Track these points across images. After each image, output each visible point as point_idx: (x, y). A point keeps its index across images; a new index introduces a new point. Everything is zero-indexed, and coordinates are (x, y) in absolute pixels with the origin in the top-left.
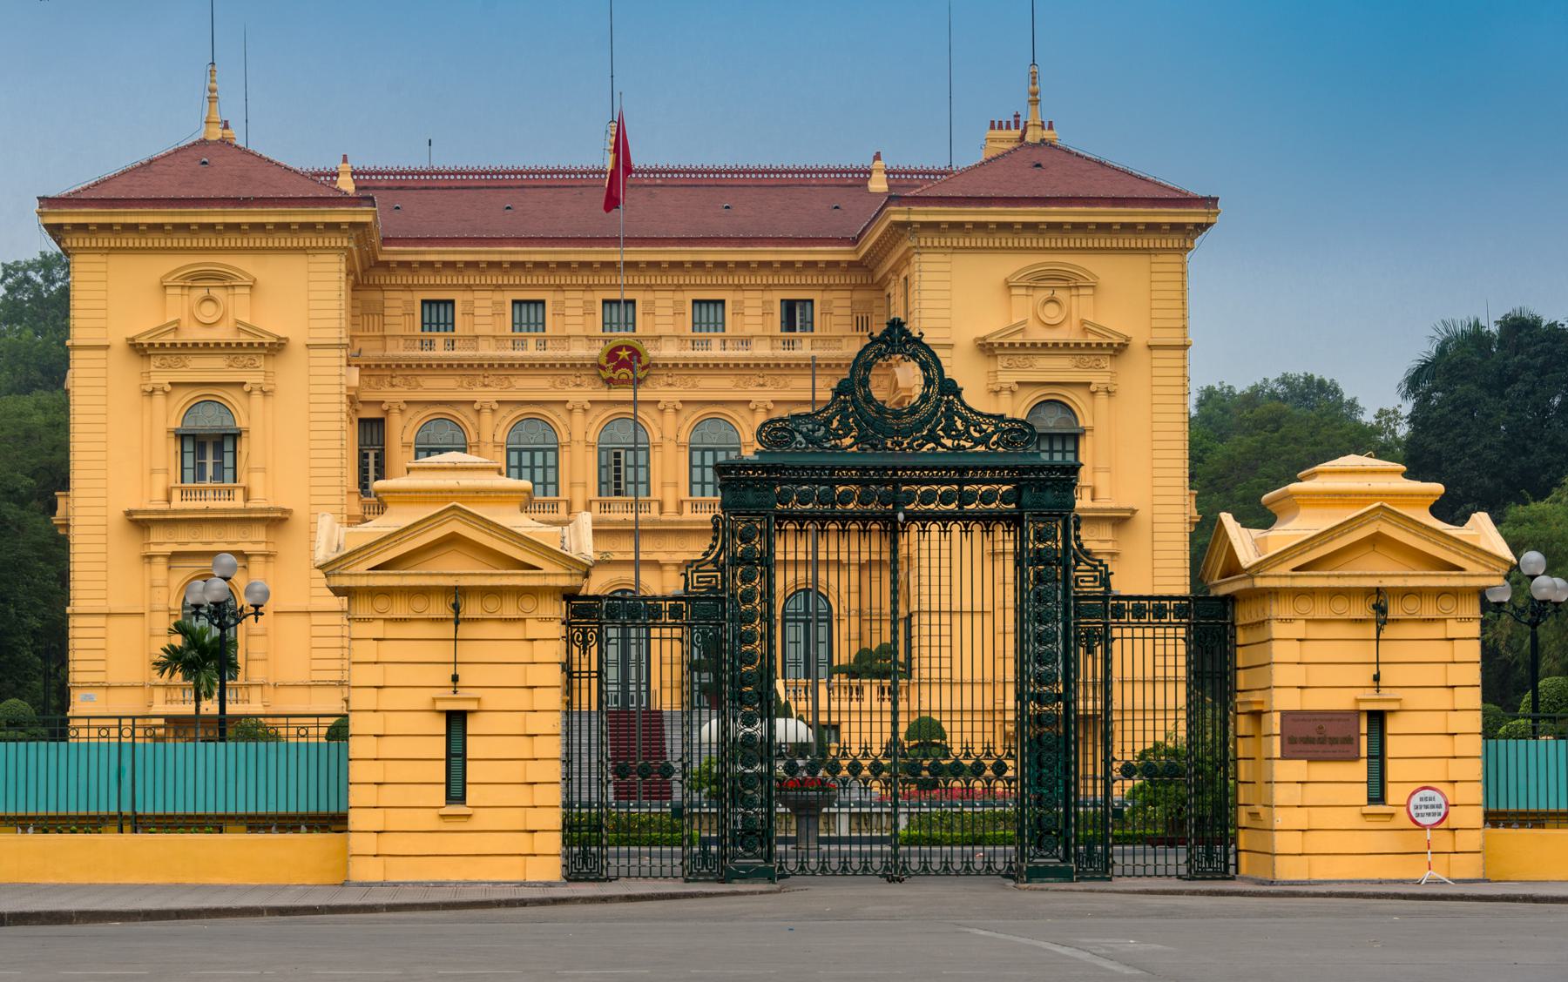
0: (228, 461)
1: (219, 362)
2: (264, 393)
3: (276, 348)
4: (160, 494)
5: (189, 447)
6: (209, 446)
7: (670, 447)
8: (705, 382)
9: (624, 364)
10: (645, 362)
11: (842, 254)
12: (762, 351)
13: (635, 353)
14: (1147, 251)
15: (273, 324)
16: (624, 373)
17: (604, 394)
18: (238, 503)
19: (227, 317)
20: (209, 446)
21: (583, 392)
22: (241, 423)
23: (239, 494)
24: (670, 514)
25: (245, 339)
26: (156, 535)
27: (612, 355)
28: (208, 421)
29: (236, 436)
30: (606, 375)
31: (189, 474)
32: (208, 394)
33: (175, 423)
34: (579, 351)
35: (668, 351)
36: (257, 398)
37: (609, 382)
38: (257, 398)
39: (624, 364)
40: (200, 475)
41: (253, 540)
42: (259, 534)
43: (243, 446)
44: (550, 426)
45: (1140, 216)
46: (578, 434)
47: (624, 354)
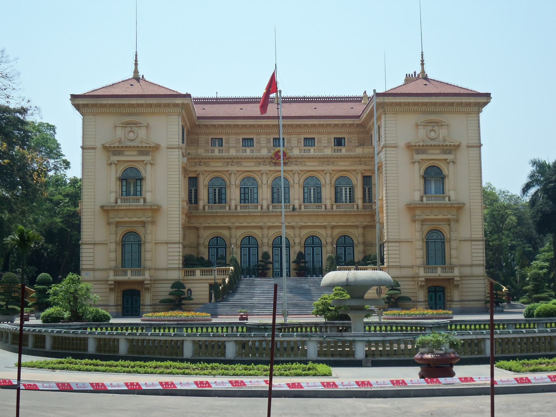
0: (139, 188)
2: (151, 164)
4: (112, 200)
5: (124, 184)
8: (308, 164)
10: (288, 156)
11: (357, 121)
12: (328, 152)
30: (274, 161)
31: (124, 193)
34: (264, 152)
35: (296, 152)
36: (149, 166)
38: (149, 166)
43: (144, 183)
44: (254, 179)
46: (265, 182)
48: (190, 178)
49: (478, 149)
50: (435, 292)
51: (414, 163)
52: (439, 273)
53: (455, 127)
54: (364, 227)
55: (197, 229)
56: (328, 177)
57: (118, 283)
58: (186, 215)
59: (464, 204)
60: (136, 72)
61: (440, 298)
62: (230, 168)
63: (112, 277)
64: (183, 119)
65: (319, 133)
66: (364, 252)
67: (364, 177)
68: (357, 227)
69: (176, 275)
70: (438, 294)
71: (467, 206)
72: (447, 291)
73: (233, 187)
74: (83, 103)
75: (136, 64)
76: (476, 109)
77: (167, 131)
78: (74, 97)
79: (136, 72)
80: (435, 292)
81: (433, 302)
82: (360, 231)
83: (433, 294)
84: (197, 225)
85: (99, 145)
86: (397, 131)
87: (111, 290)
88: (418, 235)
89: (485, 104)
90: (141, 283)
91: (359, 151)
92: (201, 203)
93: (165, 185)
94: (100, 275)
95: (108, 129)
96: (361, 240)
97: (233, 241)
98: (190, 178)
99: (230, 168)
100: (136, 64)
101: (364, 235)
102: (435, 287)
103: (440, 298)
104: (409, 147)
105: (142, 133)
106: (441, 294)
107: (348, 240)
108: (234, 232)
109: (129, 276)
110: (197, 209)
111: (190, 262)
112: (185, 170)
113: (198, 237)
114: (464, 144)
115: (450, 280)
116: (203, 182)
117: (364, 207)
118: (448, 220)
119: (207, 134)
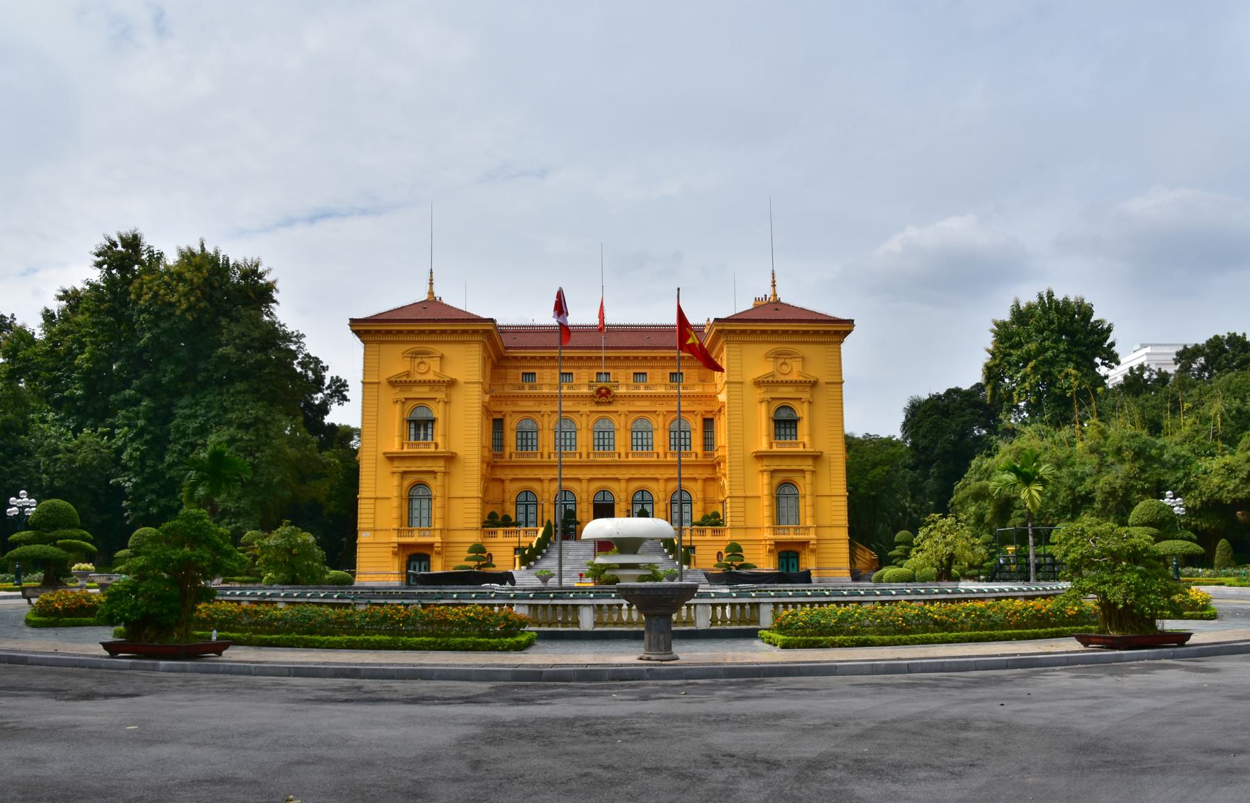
1: (426, 389)
3: (452, 383)
6: (420, 425)
7: (622, 430)
8: (638, 403)
9: (604, 395)
12: (661, 390)
13: (608, 392)
15: (451, 373)
18: (433, 449)
19: (430, 370)
20: (420, 425)
21: (587, 408)
22: (435, 415)
23: (433, 446)
24: (623, 458)
25: (436, 379)
26: (396, 464)
27: (599, 391)
28: (421, 414)
29: (433, 421)
32: (421, 402)
33: (406, 416)
34: (585, 390)
35: (622, 390)
37: (598, 403)
39: (604, 395)
40: (417, 437)
41: (439, 466)
42: (441, 463)
48: (494, 420)
50: (787, 559)
52: (791, 536)
53: (808, 361)
54: (706, 480)
55: (502, 481)
56: (661, 418)
57: (402, 546)
58: (488, 464)
60: (431, 293)
62: (543, 408)
63: (395, 539)
64: (485, 348)
65: (615, 367)
66: (704, 510)
67: (705, 420)
68: (695, 479)
69: (474, 538)
70: (791, 561)
71: (826, 455)
72: (802, 557)
73: (546, 431)
74: (366, 329)
75: (431, 284)
76: (835, 339)
77: (465, 364)
78: (353, 322)
79: (431, 293)
82: (700, 484)
84: (503, 477)
85: (383, 380)
87: (394, 554)
89: (847, 333)
90: (430, 546)
91: (698, 390)
92: (508, 451)
93: (463, 429)
94: (381, 538)
95: (396, 361)
96: (700, 495)
97: (546, 496)
98: (494, 420)
99: (543, 408)
100: (431, 284)
101: (704, 491)
102: (788, 552)
104: (758, 383)
105: (434, 364)
107: (647, 497)
108: (546, 484)
110: (502, 456)
111: (494, 521)
112: (486, 410)
113: (504, 491)
114: (823, 379)
115: (804, 544)
116: (511, 424)
117: (705, 456)
118: (803, 471)
119: (517, 368)
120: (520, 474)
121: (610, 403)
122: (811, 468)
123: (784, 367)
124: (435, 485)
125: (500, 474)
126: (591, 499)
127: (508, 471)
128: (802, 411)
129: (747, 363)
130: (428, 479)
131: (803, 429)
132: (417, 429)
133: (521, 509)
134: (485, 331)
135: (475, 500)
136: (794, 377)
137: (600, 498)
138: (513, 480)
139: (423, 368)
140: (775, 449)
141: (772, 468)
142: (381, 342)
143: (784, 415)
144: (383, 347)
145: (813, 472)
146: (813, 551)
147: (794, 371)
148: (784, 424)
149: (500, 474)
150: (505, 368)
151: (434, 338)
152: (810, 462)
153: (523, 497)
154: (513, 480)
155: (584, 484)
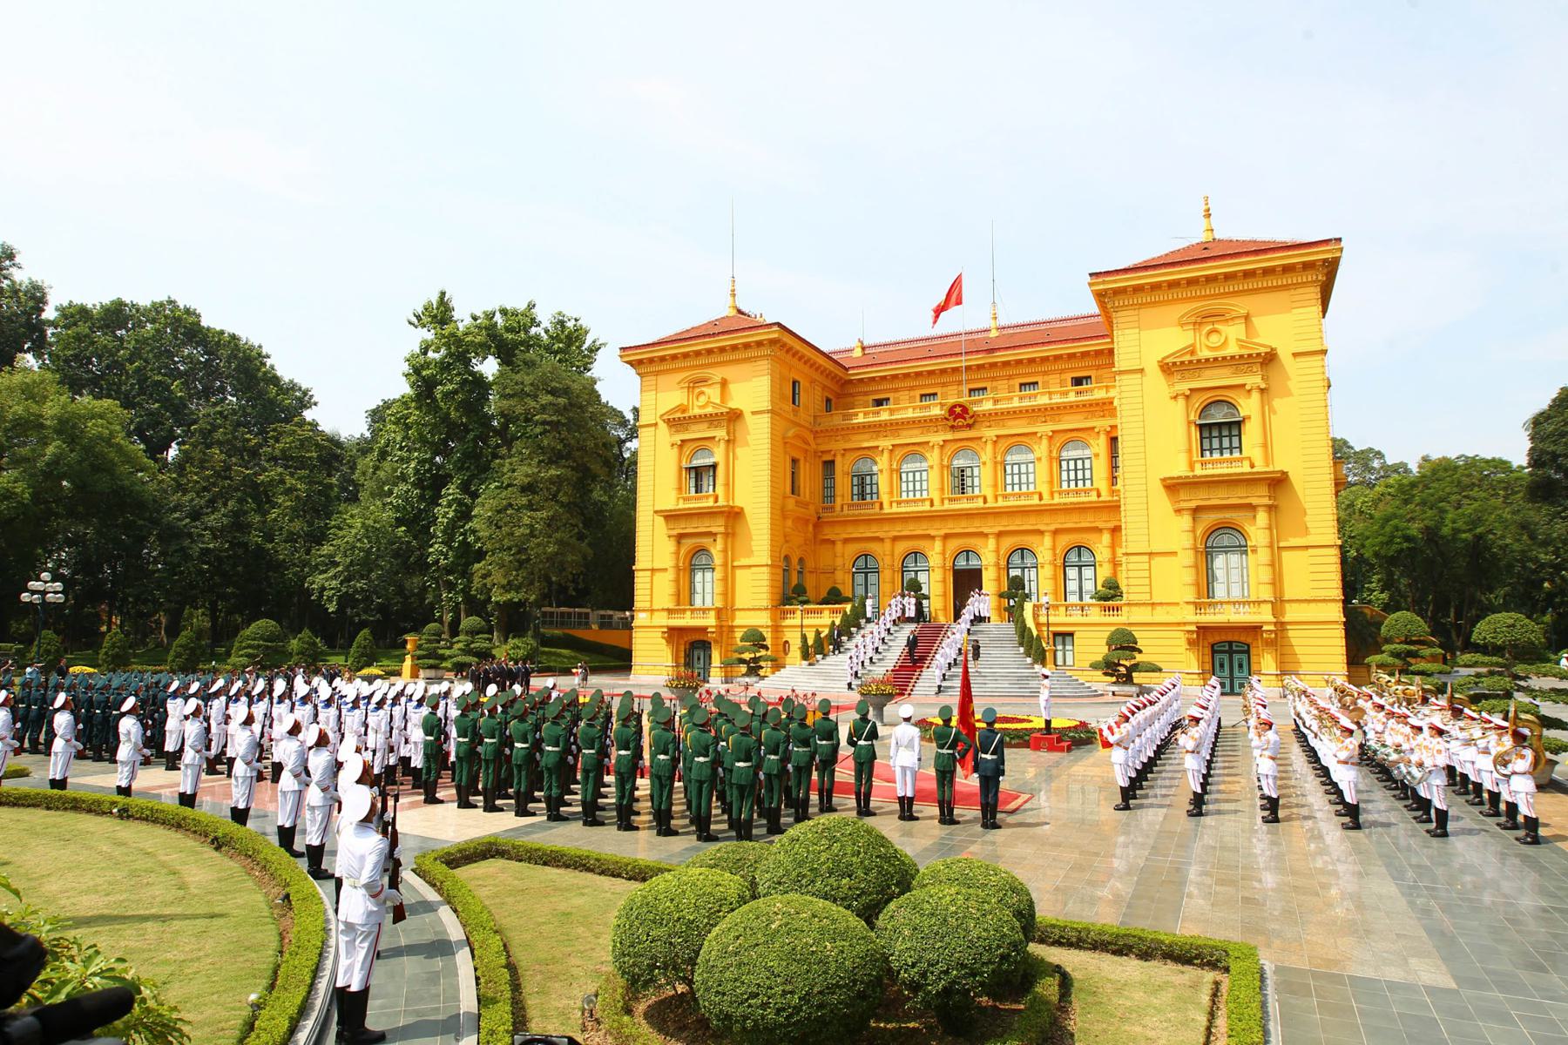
13: (965, 410)
14: (1285, 287)
16: (960, 422)
17: (949, 436)
27: (951, 411)
30: (951, 423)
32: (703, 444)
37: (952, 427)
40: (698, 489)
41: (718, 526)
45: (1277, 260)
47: (958, 410)
49: (1320, 357)
50: (1231, 652)
51: (1175, 398)
55: (833, 542)
59: (1284, 474)
61: (1241, 666)
70: (1236, 657)
72: (1253, 651)
77: (752, 390)
80: (1231, 652)
81: (1227, 673)
83: (1226, 657)
86: (1148, 341)
88: (1186, 541)
92: (839, 501)
93: (751, 478)
102: (1230, 643)
103: (1241, 666)
105: (713, 393)
106: (1244, 657)
109: (687, 621)
116: (841, 466)
120: (899, 530)
121: (969, 426)
122: (1266, 501)
123: (1214, 338)
124: (716, 550)
125: (829, 533)
126: (949, 564)
127: (838, 529)
128: (1248, 406)
129: (1148, 341)
130: (706, 541)
131: (1251, 435)
132: (698, 479)
133: (860, 578)
134: (773, 342)
135: (765, 569)
136: (1233, 350)
137: (962, 563)
138: (846, 541)
139: (703, 400)
140: (1199, 471)
141: (1193, 504)
142: (657, 373)
143: (1218, 416)
144: (661, 378)
145: (1271, 509)
146: (1271, 644)
147: (1231, 339)
148: (1218, 430)
149: (829, 533)
150: (852, 395)
151: (712, 359)
152: (1263, 490)
153: (861, 563)
154: (846, 541)
155: (888, 544)
